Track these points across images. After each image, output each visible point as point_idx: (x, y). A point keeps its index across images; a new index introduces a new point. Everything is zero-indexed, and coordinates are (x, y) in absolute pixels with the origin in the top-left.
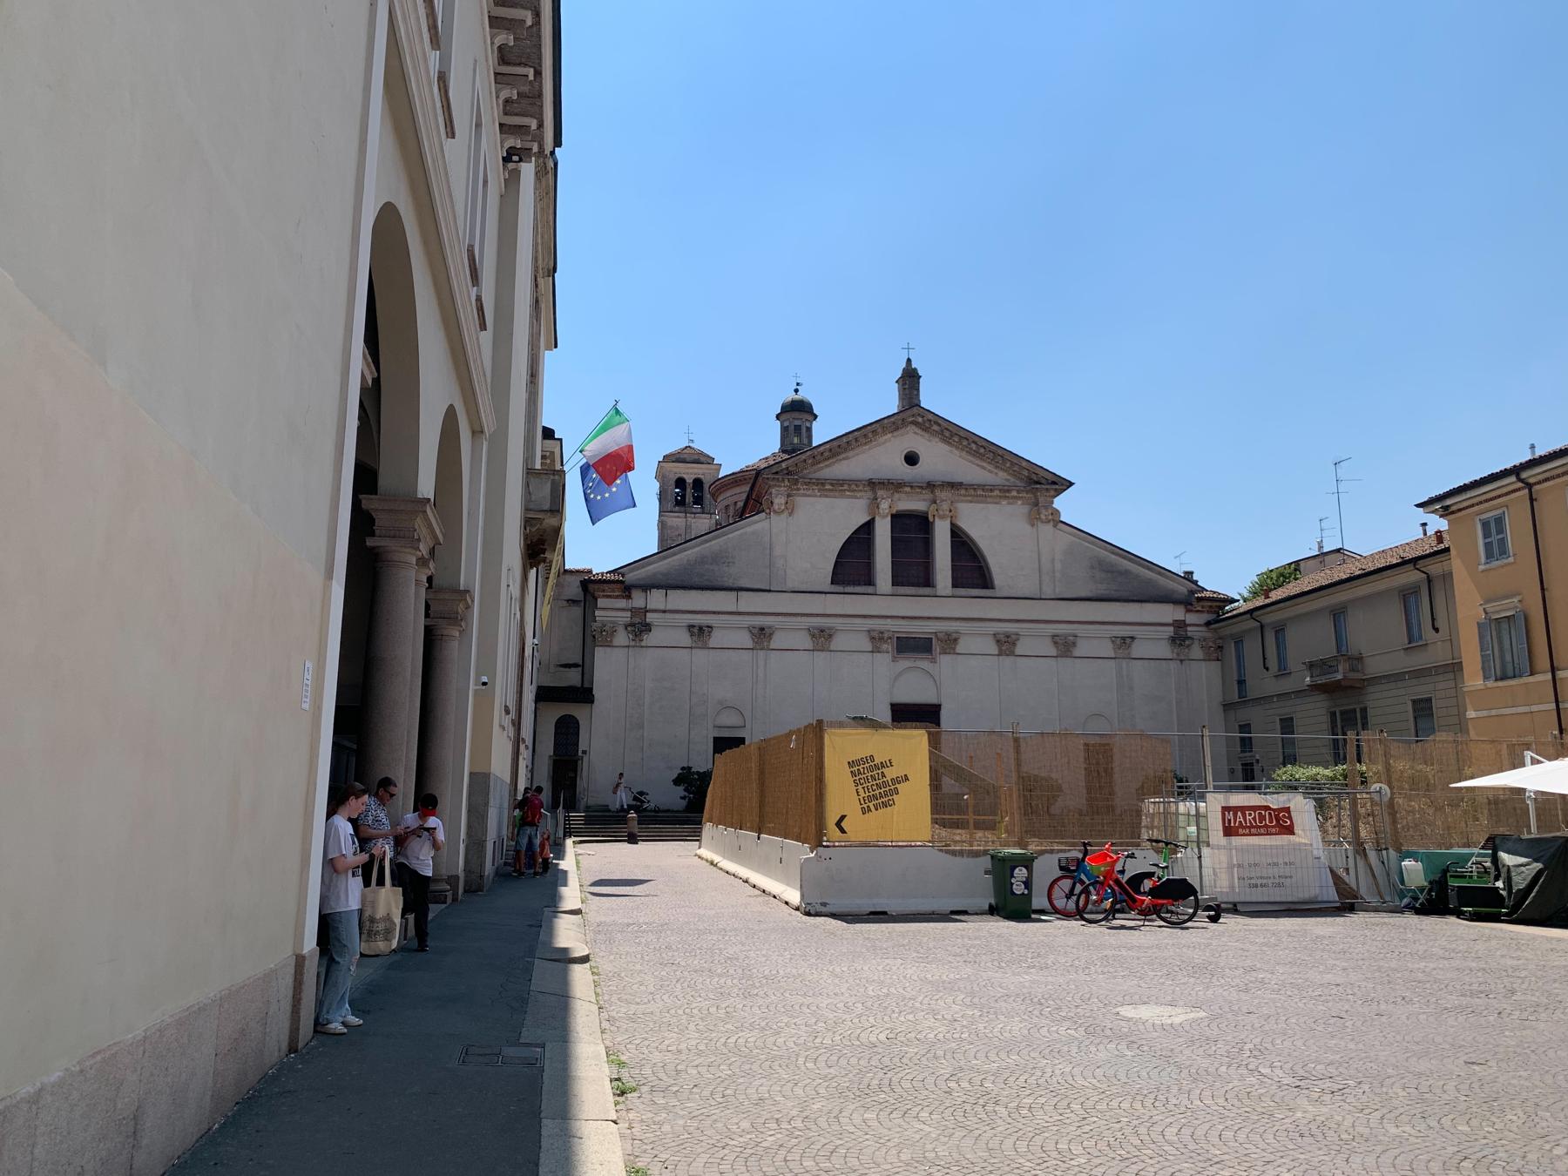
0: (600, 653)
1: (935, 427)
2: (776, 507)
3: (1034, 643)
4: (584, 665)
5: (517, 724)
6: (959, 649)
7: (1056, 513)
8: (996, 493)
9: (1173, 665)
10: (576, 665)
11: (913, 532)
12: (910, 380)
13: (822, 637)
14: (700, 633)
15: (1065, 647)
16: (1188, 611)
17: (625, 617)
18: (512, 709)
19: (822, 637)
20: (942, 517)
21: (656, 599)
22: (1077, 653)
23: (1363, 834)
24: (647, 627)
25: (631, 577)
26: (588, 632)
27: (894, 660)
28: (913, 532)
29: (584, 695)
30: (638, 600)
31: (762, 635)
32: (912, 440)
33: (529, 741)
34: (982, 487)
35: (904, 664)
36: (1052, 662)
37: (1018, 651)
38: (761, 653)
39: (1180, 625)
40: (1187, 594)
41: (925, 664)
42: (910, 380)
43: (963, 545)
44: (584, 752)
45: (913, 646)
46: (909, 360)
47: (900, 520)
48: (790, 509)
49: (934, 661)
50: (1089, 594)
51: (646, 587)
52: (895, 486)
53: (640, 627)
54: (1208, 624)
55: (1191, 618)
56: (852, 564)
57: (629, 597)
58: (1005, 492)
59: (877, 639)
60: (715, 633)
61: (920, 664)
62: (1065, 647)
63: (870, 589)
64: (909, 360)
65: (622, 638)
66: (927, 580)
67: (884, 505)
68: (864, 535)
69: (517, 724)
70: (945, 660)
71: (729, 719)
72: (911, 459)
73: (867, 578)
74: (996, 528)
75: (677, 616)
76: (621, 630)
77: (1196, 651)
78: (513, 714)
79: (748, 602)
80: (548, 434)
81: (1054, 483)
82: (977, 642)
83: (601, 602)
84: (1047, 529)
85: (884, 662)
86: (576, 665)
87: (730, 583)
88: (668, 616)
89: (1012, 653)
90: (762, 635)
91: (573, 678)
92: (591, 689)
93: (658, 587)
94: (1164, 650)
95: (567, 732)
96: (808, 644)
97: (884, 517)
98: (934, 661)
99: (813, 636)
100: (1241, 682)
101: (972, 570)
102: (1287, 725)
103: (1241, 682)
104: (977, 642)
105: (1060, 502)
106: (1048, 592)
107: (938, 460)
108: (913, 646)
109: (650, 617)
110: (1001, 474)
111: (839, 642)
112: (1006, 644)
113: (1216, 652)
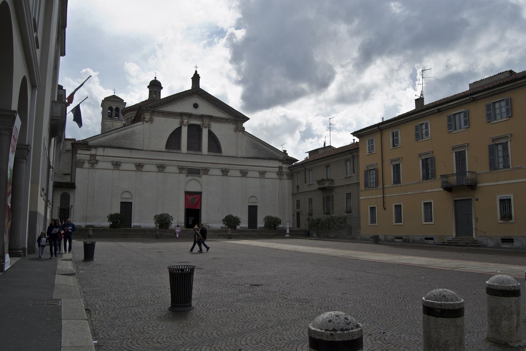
0: (78, 171)
1: (205, 96)
2: (146, 119)
4: (72, 175)
5: (47, 195)
6: (209, 173)
7: (244, 128)
9: (278, 181)
10: (69, 174)
11: (195, 132)
12: (196, 78)
14: (117, 165)
15: (244, 174)
16: (283, 163)
17: (88, 157)
18: (45, 189)
19: (161, 168)
20: (205, 127)
22: (248, 176)
23: (333, 236)
24: (97, 162)
25: (90, 143)
26: (74, 163)
27: (187, 176)
28: (195, 132)
29: (72, 186)
30: (93, 152)
31: (139, 167)
32: (196, 100)
33: (51, 201)
35: (190, 178)
36: (240, 178)
37: (229, 175)
38: (139, 173)
39: (280, 168)
40: (285, 159)
41: (197, 178)
42: (196, 78)
43: (212, 137)
44: (72, 206)
45: (194, 172)
46: (196, 72)
47: (191, 127)
48: (151, 120)
49: (200, 177)
51: (96, 147)
52: (190, 116)
53: (93, 161)
54: (289, 168)
55: (284, 166)
56: (173, 142)
57: (90, 150)
59: (181, 169)
61: (195, 178)
62: (244, 174)
63: (179, 151)
64: (196, 72)
65: (86, 165)
66: (199, 148)
67: (185, 121)
68: (177, 133)
69: (47, 195)
70: (204, 177)
71: (126, 195)
72: (196, 106)
73: (179, 148)
74: (223, 131)
76: (86, 162)
77: (285, 177)
78: (45, 191)
79: (134, 154)
80: (61, 87)
81: (243, 118)
83: (79, 152)
84: (240, 134)
85: (183, 177)
86: (69, 174)
87: (128, 146)
88: (105, 157)
89: (227, 175)
90: (139, 167)
91: (67, 179)
92: (74, 184)
93: (101, 146)
94: (275, 176)
95: (65, 199)
96: (156, 170)
97: (185, 126)
98: (200, 177)
100: (298, 187)
101: (215, 145)
102: (311, 201)
103: (298, 187)
105: (245, 125)
106: (240, 155)
108: (194, 172)
111: (168, 169)
112: (225, 172)
113: (291, 176)
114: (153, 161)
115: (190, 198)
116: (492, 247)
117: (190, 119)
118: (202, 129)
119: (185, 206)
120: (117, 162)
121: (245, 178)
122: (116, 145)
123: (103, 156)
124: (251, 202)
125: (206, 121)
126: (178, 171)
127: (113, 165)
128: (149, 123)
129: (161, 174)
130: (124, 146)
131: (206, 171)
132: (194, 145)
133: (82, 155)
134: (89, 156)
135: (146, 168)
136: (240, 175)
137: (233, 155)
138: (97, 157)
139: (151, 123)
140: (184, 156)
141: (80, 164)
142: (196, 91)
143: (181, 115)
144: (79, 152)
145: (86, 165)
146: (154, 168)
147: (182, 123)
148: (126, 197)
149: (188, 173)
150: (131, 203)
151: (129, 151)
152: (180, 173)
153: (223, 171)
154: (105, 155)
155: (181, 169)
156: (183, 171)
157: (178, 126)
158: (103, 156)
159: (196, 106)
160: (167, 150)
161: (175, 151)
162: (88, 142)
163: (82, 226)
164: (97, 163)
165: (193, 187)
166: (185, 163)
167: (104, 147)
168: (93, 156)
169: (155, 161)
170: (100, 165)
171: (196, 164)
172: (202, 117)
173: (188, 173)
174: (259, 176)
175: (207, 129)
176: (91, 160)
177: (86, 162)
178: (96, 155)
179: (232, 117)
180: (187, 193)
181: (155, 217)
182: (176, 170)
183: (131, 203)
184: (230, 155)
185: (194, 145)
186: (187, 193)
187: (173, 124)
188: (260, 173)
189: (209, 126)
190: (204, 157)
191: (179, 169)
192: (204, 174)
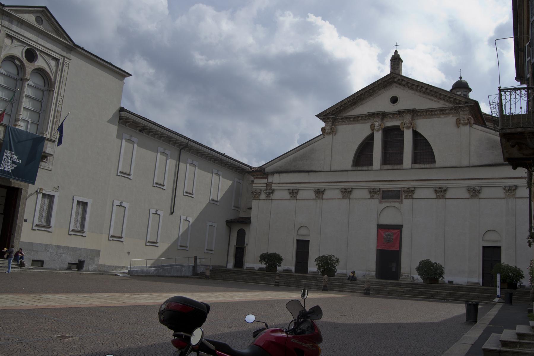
3: (307, 194)
8: (447, 111)
12: (396, 61)
13: (347, 193)
14: (294, 193)
17: (263, 187)
19: (347, 193)
20: (408, 128)
21: (275, 179)
24: (273, 191)
25: (267, 170)
28: (393, 136)
29: (247, 221)
30: (270, 179)
31: (319, 193)
32: (395, 91)
34: (427, 111)
38: (318, 201)
41: (396, 204)
42: (396, 61)
50: (491, 163)
51: (272, 173)
52: (383, 115)
53: (270, 191)
56: (363, 156)
58: (441, 112)
59: (373, 192)
60: (300, 193)
62: (475, 193)
63: (370, 168)
64: (396, 52)
65: (263, 196)
67: (377, 124)
68: (368, 143)
70: (407, 202)
71: (303, 231)
75: (284, 185)
79: (313, 178)
81: (466, 103)
82: (425, 193)
85: (375, 204)
87: (306, 169)
88: (281, 185)
89: (443, 197)
90: (319, 193)
92: (249, 218)
95: (241, 235)
96: (340, 196)
97: (378, 130)
98: (401, 202)
99: (342, 191)
104: (425, 193)
106: (465, 163)
107: (408, 100)
108: (391, 196)
109: (274, 186)
110: (442, 102)
112: (441, 193)
114: (336, 184)
115: (384, 234)
116: (92, 271)
117: (385, 120)
118: (403, 131)
119: (378, 246)
120: (293, 190)
121: (476, 201)
122: (293, 169)
123: (279, 183)
124: (489, 241)
125: (407, 119)
126: (369, 196)
127: (290, 193)
128: (331, 136)
129: (346, 201)
130: (302, 169)
131: (410, 193)
132: (392, 157)
133: (260, 184)
134: (265, 185)
135: (327, 195)
136: (467, 195)
137: (454, 164)
138: (273, 185)
139: (335, 135)
140: (378, 173)
141: (256, 195)
142: (395, 78)
143: (372, 115)
144: (256, 181)
145: (263, 196)
146: (337, 194)
147: (372, 126)
148: (303, 234)
149: (383, 198)
150: (309, 241)
151: (307, 174)
152: (372, 198)
153: (436, 191)
154: (281, 182)
155: (373, 192)
156: (376, 196)
157: (368, 132)
158: (279, 183)
159: (394, 100)
160: (354, 168)
161: (364, 168)
162: (265, 169)
163: (255, 268)
164: (272, 193)
165: (390, 218)
166: (378, 183)
167: (280, 172)
168: (268, 184)
169: (338, 184)
170: (277, 195)
171: (394, 183)
172: (400, 113)
173: (383, 198)
174: (503, 196)
175: (411, 130)
176: (266, 190)
177: (263, 193)
178: (272, 183)
179: (451, 105)
180: (380, 227)
181: (338, 261)
182: (367, 195)
183: (309, 241)
184: (449, 165)
185: (392, 157)
186: (380, 227)
187: (362, 131)
188: (504, 189)
189: (411, 125)
190: (407, 172)
191: (370, 192)
192: (406, 198)
